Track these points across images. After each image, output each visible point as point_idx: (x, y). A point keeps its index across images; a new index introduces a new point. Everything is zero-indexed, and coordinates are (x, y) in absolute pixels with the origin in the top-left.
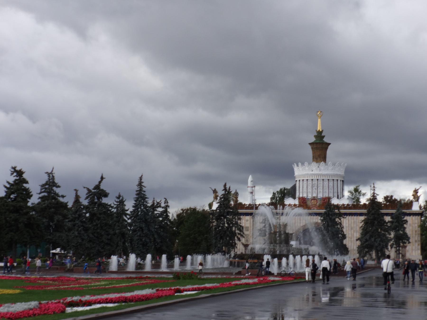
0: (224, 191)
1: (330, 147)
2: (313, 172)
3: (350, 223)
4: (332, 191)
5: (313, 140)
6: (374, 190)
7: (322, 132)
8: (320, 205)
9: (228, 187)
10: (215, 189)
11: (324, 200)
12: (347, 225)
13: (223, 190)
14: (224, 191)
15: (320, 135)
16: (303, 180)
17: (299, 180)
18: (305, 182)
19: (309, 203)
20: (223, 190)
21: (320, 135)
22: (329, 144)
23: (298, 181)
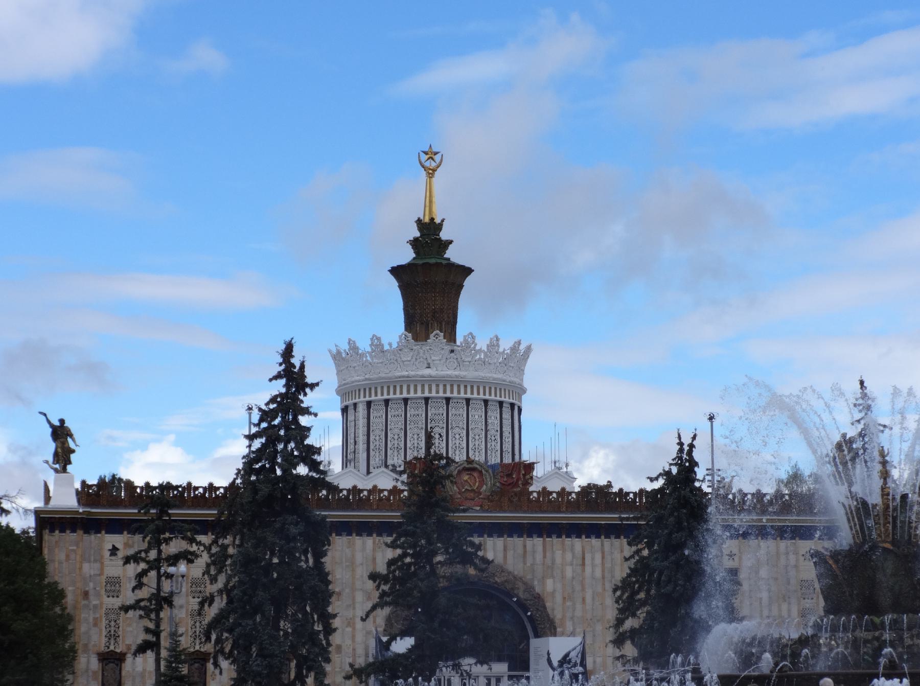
0: (283, 381)
1: (469, 282)
3: (608, 565)
4: (498, 448)
5: (407, 255)
6: (869, 408)
7: (439, 227)
8: (493, 493)
9: (296, 361)
10: (62, 421)
11: (509, 475)
12: (598, 573)
13: (278, 377)
14: (283, 381)
15: (429, 238)
16: (387, 402)
17: (369, 404)
18: (396, 411)
20: (278, 377)
21: (429, 238)
22: (467, 271)
23: (362, 409)
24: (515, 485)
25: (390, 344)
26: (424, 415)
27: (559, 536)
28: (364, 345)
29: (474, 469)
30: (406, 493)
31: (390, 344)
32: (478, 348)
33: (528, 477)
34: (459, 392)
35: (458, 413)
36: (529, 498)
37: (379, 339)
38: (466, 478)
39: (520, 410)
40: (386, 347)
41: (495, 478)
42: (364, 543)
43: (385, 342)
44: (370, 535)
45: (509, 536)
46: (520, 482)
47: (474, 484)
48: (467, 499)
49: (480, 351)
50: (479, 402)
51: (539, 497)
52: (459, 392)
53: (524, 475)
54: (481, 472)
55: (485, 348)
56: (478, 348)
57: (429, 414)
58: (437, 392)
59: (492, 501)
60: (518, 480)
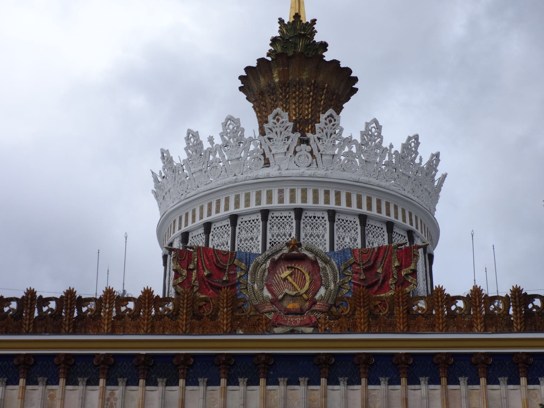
2: (272, 171)
8: (337, 300)
11: (370, 269)
19: (258, 290)
25: (211, 140)
26: (260, 238)
27: (473, 381)
28: (179, 154)
29: (302, 258)
31: (211, 140)
32: (345, 135)
34: (316, 200)
35: (315, 232)
36: (409, 311)
37: (196, 135)
38: (286, 273)
39: (431, 258)
40: (206, 145)
41: (343, 275)
42: (84, 399)
43: (204, 138)
44: (92, 382)
45: (370, 382)
46: (391, 281)
47: (302, 287)
48: (289, 312)
49: (349, 141)
50: (350, 218)
51: (430, 308)
52: (316, 200)
53: (399, 268)
54: (314, 263)
55: (357, 137)
56: (345, 135)
57: (269, 236)
58: (281, 201)
59: (338, 317)
60: (386, 279)
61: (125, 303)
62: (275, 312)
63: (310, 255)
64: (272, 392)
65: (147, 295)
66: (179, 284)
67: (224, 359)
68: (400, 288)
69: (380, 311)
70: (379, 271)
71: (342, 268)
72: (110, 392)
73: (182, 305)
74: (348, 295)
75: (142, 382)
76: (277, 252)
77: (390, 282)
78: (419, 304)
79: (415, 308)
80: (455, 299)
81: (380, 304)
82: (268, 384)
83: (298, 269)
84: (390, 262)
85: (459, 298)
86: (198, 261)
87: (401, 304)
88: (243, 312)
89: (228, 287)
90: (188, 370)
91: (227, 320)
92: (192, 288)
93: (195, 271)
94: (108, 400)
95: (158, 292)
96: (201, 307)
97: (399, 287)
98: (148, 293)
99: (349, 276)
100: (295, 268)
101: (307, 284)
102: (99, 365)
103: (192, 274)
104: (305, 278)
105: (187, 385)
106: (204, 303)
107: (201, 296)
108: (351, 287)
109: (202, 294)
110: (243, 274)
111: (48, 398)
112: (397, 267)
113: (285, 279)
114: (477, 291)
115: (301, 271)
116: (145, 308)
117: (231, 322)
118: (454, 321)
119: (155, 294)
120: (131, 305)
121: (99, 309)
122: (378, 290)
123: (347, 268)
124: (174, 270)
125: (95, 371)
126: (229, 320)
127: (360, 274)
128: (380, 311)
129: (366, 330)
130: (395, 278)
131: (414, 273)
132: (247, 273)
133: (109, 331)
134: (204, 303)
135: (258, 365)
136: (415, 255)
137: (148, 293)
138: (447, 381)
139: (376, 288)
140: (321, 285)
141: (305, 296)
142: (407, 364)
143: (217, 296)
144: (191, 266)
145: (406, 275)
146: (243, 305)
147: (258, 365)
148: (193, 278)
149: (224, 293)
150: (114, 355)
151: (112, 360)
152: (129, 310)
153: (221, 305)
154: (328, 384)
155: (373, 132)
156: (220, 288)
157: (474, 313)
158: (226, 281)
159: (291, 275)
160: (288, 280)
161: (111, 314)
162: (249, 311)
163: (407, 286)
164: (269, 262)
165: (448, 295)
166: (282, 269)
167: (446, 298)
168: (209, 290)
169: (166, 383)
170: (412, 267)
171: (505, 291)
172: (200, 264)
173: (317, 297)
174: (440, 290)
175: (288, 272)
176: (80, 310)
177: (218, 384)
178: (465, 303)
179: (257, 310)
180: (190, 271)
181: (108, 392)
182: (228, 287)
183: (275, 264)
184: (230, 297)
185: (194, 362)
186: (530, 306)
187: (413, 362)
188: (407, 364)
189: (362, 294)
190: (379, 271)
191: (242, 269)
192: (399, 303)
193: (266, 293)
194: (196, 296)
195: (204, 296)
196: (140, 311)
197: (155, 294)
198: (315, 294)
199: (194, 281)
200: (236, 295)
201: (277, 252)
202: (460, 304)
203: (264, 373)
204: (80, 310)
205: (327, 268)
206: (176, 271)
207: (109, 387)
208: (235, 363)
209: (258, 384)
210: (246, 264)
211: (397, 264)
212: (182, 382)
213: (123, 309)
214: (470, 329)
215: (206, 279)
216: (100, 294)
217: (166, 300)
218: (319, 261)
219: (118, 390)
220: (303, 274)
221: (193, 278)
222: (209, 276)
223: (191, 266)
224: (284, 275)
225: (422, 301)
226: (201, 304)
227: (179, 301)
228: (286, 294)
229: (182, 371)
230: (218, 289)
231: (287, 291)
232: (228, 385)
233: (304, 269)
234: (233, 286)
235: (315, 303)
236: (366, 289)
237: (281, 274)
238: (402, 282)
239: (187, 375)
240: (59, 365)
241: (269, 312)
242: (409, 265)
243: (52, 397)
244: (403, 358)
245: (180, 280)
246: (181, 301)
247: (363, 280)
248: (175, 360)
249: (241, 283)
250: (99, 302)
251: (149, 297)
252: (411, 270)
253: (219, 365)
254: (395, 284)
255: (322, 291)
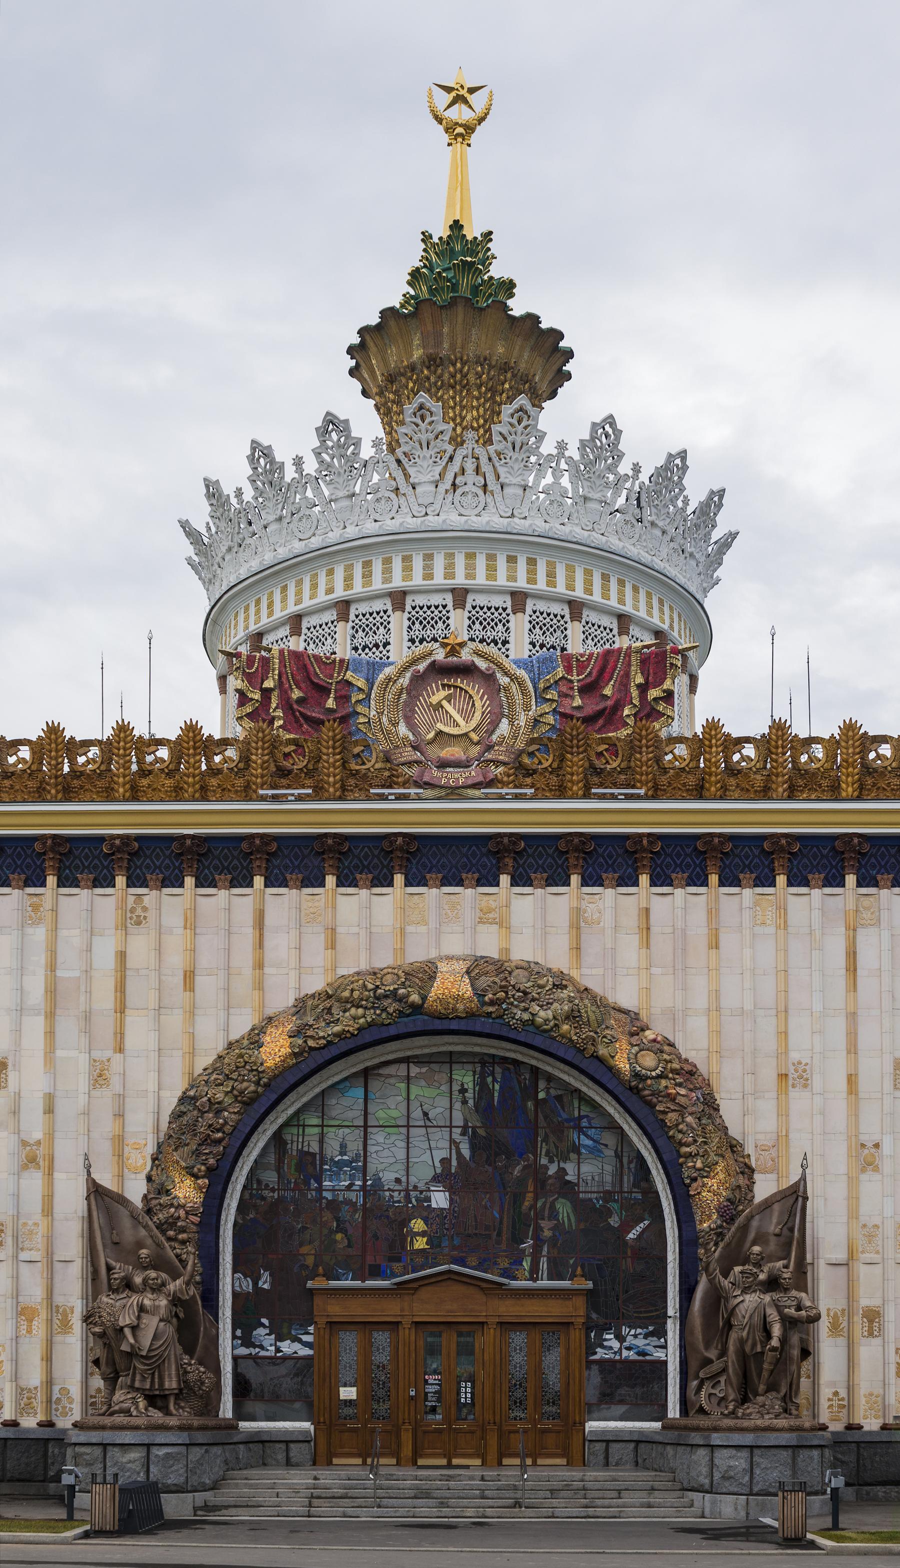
24: (609, 716)
29: (467, 670)
30: (231, 753)
33: (653, 693)
38: (439, 695)
51: (695, 758)
53: (643, 689)
60: (618, 707)
61: (152, 748)
62: (418, 762)
63: (482, 664)
64: (416, 897)
65: (191, 734)
66: (248, 715)
67: (330, 842)
68: (644, 722)
69: (607, 762)
70: (608, 691)
71: (541, 686)
72: (133, 898)
73: (254, 751)
74: (550, 734)
75: (189, 881)
76: (423, 657)
77: (626, 712)
78: (676, 751)
79: (669, 757)
80: (741, 741)
81: (606, 750)
82: (408, 883)
83: (461, 689)
84: (627, 675)
85: (747, 740)
86: (280, 675)
87: (644, 749)
88: (364, 763)
89: (335, 721)
90: (268, 860)
91: (335, 776)
92: (272, 721)
93: (276, 693)
94: (133, 910)
95: (212, 728)
96: (287, 756)
97: (641, 720)
98: (192, 729)
99: (553, 701)
100: (456, 687)
101: (478, 715)
102: (113, 854)
103: (270, 699)
104: (473, 705)
105: (266, 886)
106: (293, 748)
107: (288, 736)
108: (555, 720)
109: (290, 732)
110: (361, 696)
111: (30, 909)
112: (639, 686)
113: (439, 706)
114: (779, 728)
115: (466, 692)
116: (188, 755)
117: (342, 780)
118: (737, 782)
119: (206, 732)
120: (163, 753)
121: (106, 759)
122: (604, 726)
123: (548, 688)
124: (237, 690)
125: (106, 864)
126: (338, 777)
127: (572, 697)
128: (607, 762)
129: (581, 793)
130: (635, 706)
131: (669, 697)
132: (369, 696)
133: (128, 794)
134: (293, 748)
135: (391, 852)
136: (672, 664)
137: (192, 729)
138: (720, 880)
139: (601, 722)
140: (502, 715)
141: (475, 737)
142: (652, 853)
143: (315, 735)
144: (269, 684)
145: (655, 699)
146: (363, 751)
147: (391, 852)
148: (274, 705)
149: (326, 732)
150: (139, 838)
151: (136, 844)
152: (162, 760)
153: (324, 750)
154: (512, 885)
155: (605, 437)
156: (322, 722)
157: (772, 767)
158: (331, 711)
159: (448, 698)
160: (442, 707)
161: (129, 768)
162: (373, 761)
163: (657, 719)
164: (408, 675)
165: (729, 735)
166: (432, 688)
167: (725, 740)
168: (301, 726)
169: (231, 882)
170: (667, 684)
171: (828, 729)
172: (284, 680)
173: (494, 737)
174: (713, 726)
175: (443, 693)
176: (73, 762)
177: (322, 884)
178: (757, 748)
179: (387, 760)
180: (266, 693)
181: (131, 899)
182: (335, 721)
183: (419, 680)
184: (338, 737)
185: (279, 848)
186: (872, 755)
187: (662, 848)
188: (652, 853)
189: (575, 733)
190: (608, 691)
191: (360, 689)
192: (641, 748)
193: (403, 729)
194: (278, 736)
195: (292, 736)
196: (180, 763)
197: (206, 732)
198: (493, 732)
199: (274, 710)
200: (350, 733)
201: (423, 657)
202: (749, 750)
203: (400, 866)
204: (73, 762)
205: (514, 687)
206: (241, 693)
207: (133, 890)
208: (349, 849)
209: (390, 884)
210: (367, 680)
211: (640, 679)
212: (259, 881)
213: (149, 758)
214: (765, 793)
215: (295, 706)
216: (108, 733)
217: (225, 742)
218: (498, 675)
219: (150, 896)
220: (471, 697)
221: (274, 705)
222: (300, 701)
223: (269, 684)
224: (434, 700)
225: (683, 746)
226: (287, 750)
227: (249, 743)
228: (440, 733)
229: (258, 863)
230: (317, 723)
231: (440, 726)
232: (338, 886)
233: (473, 688)
234: (344, 720)
235: (489, 748)
236: (583, 723)
237: (429, 697)
238: (649, 713)
239: (267, 869)
240: (44, 854)
241: (410, 764)
242: (662, 683)
243: (36, 908)
244: (645, 842)
245: (249, 709)
246: (254, 745)
247: (578, 708)
248: (244, 845)
249: (358, 714)
250: (106, 746)
251: (195, 736)
252: (664, 691)
253: (323, 853)
254: (635, 715)
255: (504, 727)
